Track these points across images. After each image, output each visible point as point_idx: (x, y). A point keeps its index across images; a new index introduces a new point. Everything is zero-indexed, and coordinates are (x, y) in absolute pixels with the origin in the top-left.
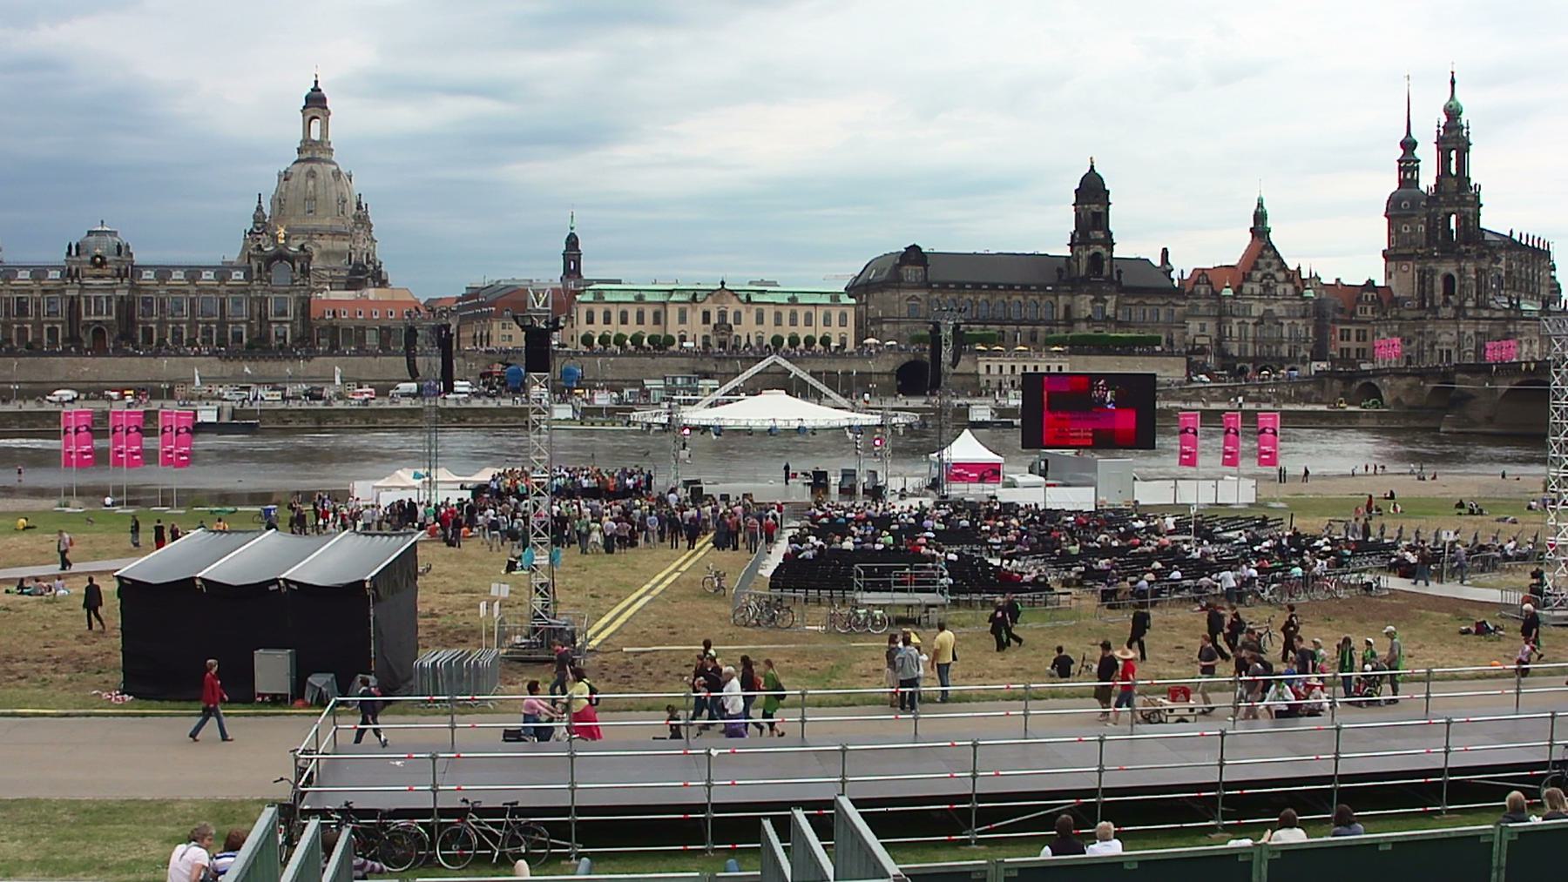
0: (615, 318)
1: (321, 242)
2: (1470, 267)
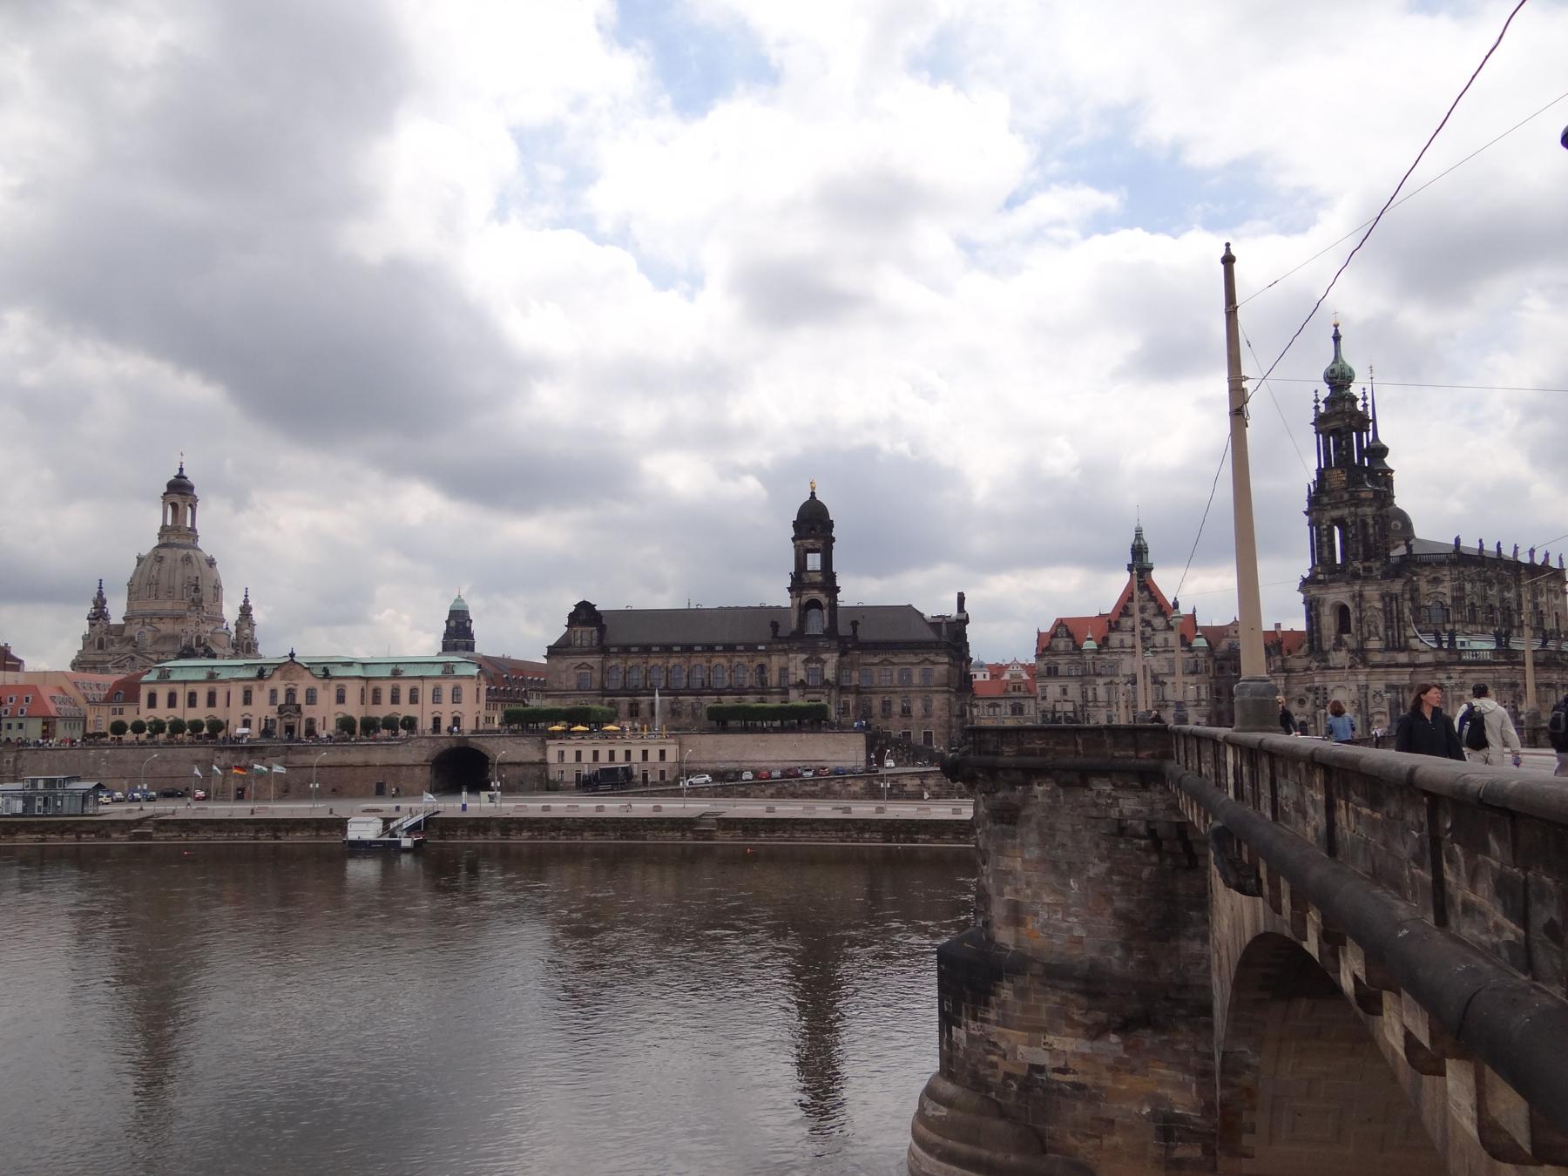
0: (181, 700)
2: (1372, 592)
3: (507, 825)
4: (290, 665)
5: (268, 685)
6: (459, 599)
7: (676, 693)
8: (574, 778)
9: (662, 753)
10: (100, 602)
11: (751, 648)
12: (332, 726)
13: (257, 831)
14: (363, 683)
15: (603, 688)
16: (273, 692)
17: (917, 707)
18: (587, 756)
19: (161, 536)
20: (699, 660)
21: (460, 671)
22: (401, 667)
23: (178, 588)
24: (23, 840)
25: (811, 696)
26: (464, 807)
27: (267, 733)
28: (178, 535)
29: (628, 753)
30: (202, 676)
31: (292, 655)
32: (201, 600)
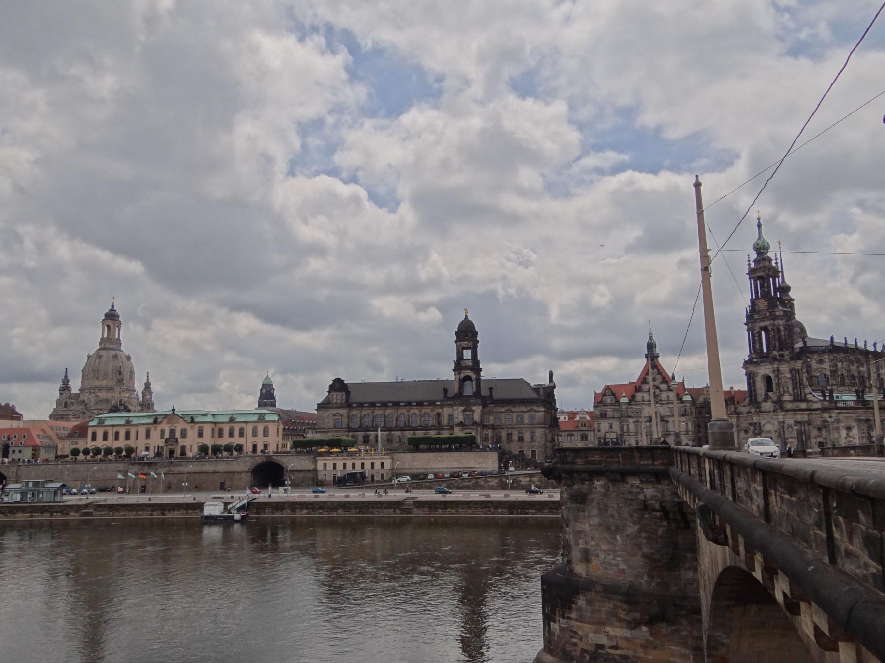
0: (111, 436)
1: (100, 394)
2: (784, 368)
3: (294, 506)
4: (172, 416)
5: (160, 427)
6: (267, 378)
7: (390, 430)
8: (332, 479)
9: (382, 464)
10: (66, 381)
11: (432, 403)
12: (195, 450)
13: (152, 511)
14: (213, 425)
15: (348, 427)
16: (163, 432)
17: (527, 436)
18: (340, 466)
19: (101, 344)
20: (403, 411)
21: (267, 418)
22: (235, 416)
23: (110, 372)
24: (20, 517)
25: (467, 431)
26: (270, 496)
27: (159, 454)
28: (110, 343)
29: (363, 464)
30: (123, 422)
31: (173, 410)
32: (123, 380)
